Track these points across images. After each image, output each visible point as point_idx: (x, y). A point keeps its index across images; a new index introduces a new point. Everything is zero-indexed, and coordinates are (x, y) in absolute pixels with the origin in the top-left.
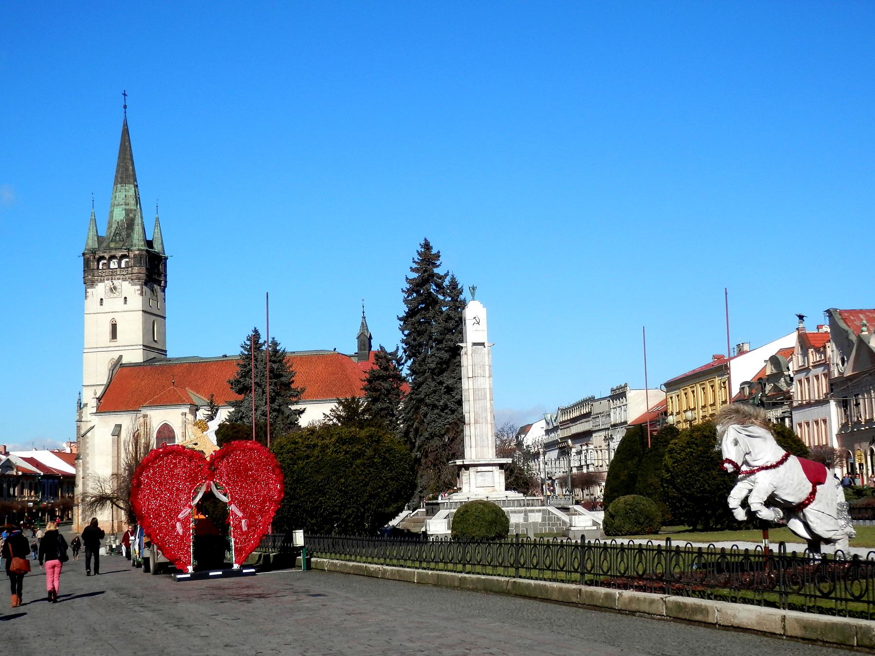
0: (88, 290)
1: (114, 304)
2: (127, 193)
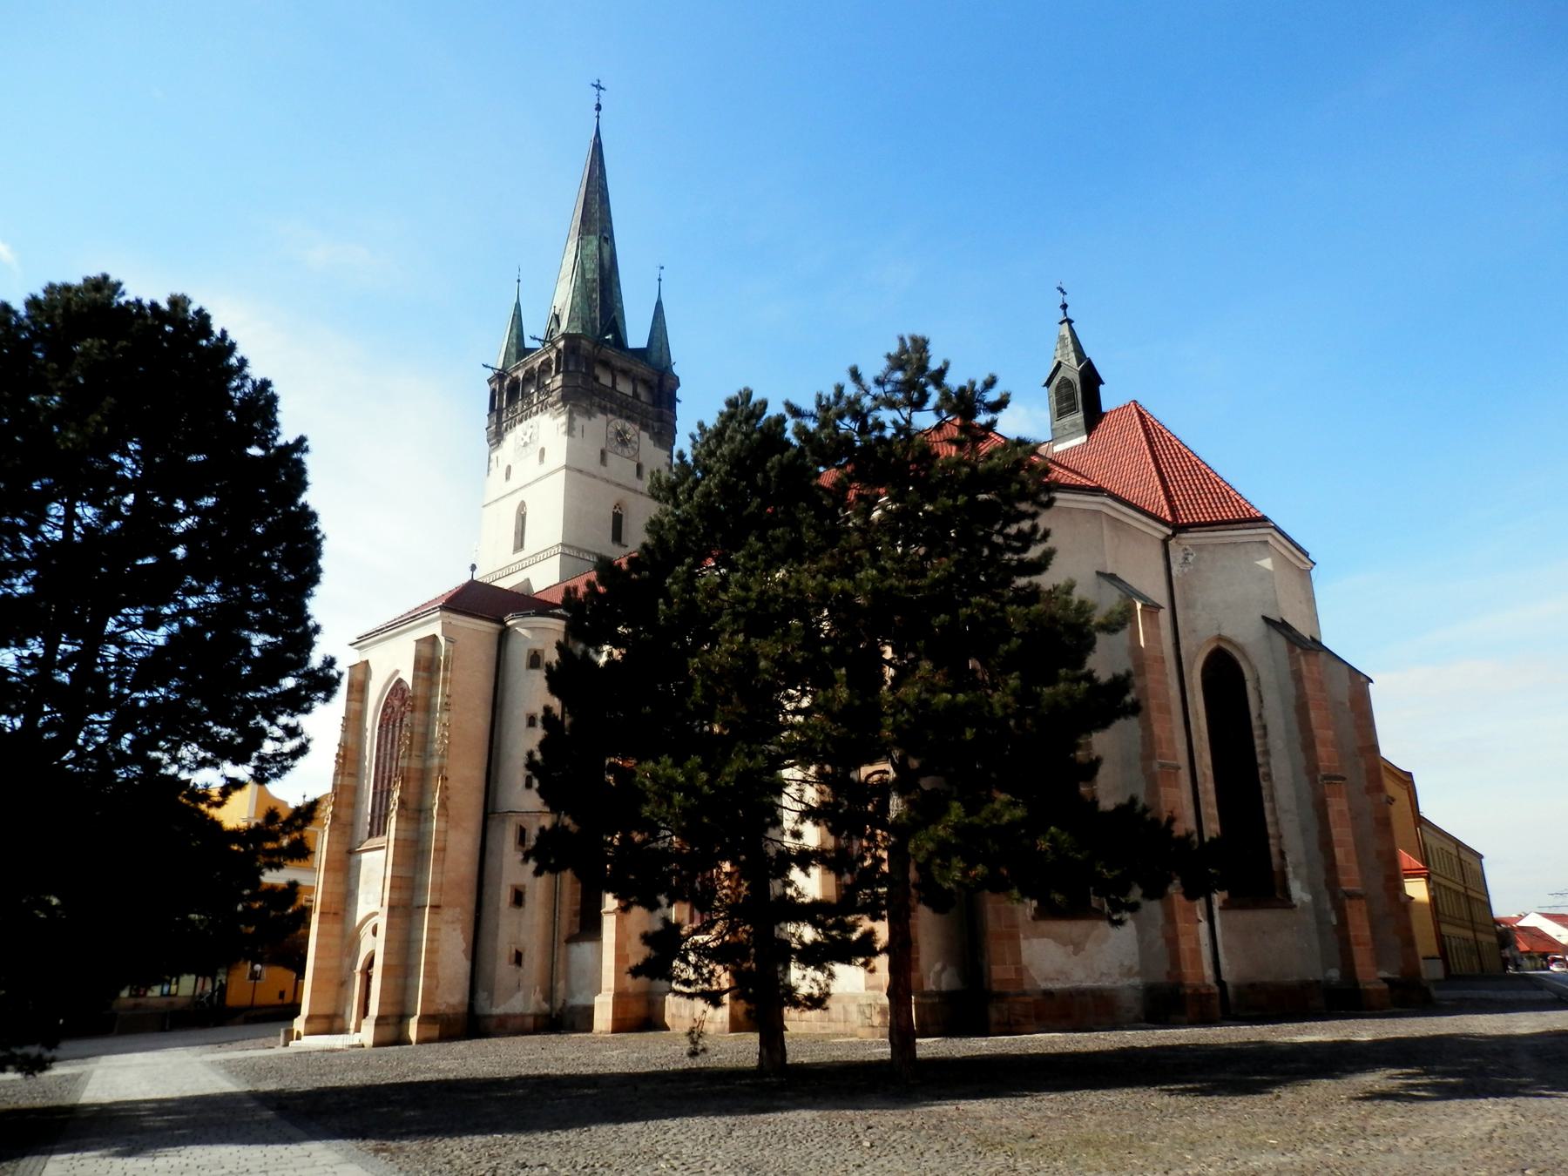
1: (526, 468)
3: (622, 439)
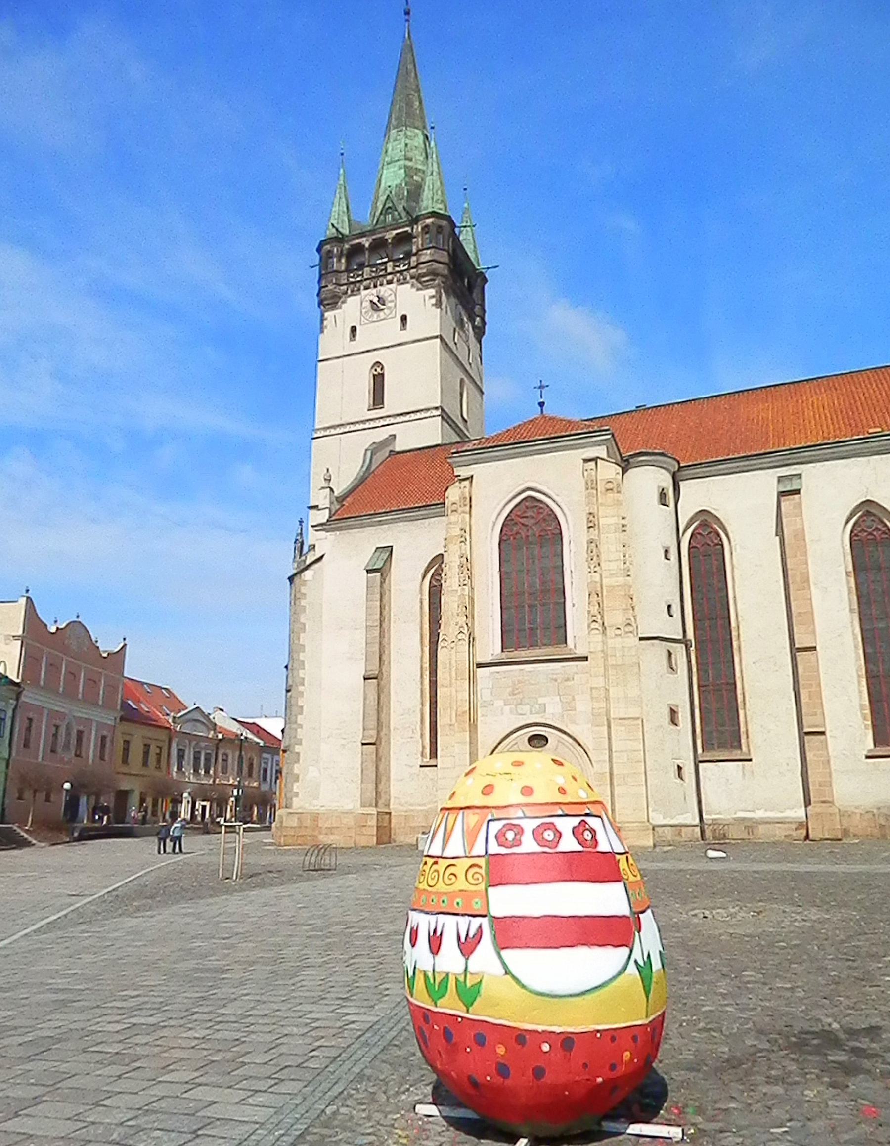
0: (326, 315)
2: (408, 141)
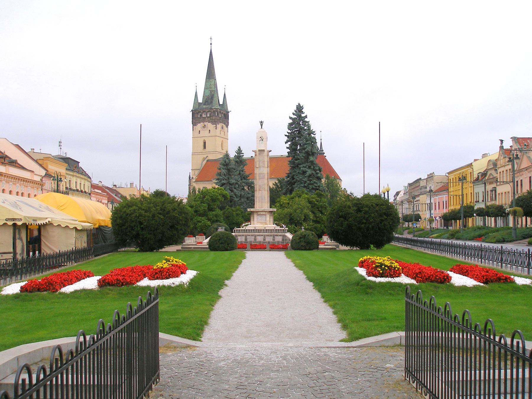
0: (194, 127)
1: (205, 133)
3: (222, 128)
